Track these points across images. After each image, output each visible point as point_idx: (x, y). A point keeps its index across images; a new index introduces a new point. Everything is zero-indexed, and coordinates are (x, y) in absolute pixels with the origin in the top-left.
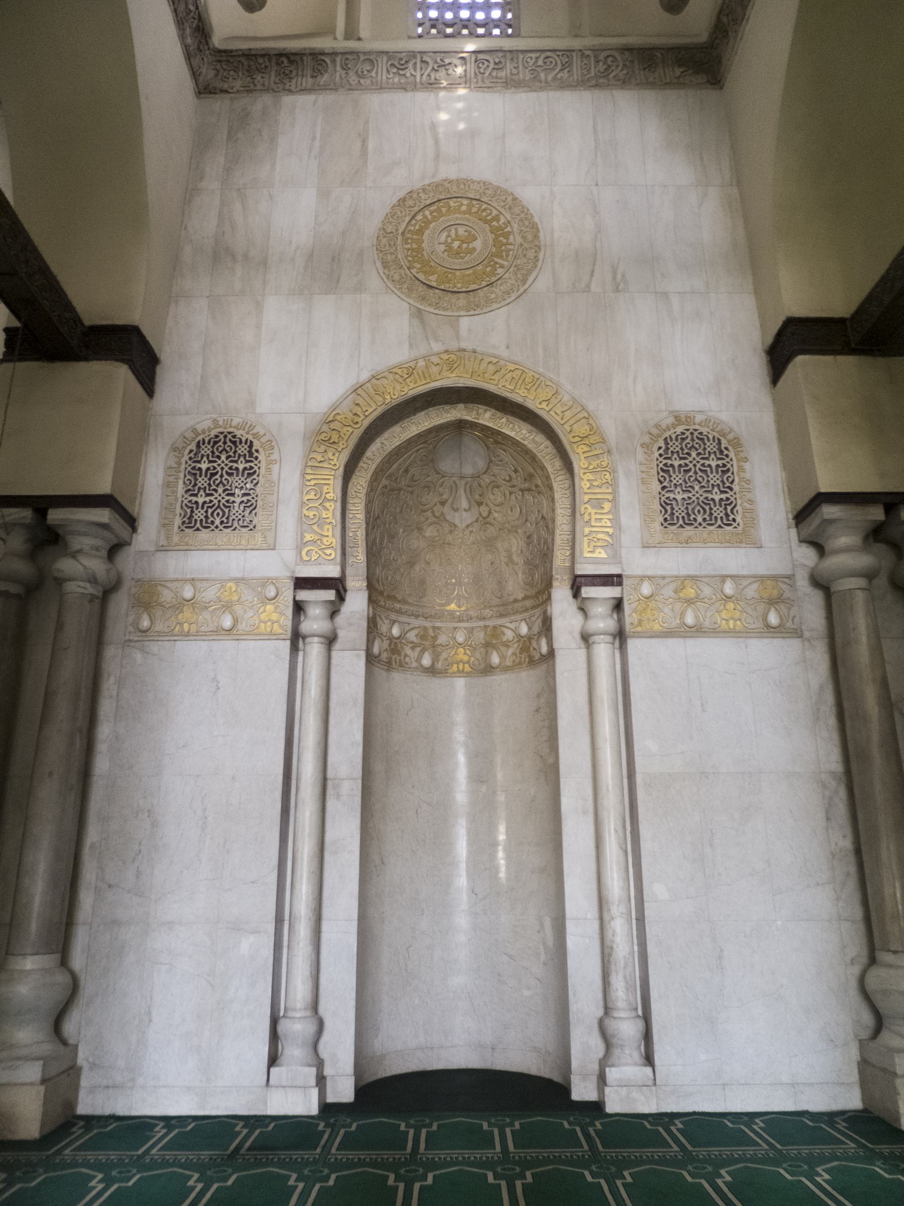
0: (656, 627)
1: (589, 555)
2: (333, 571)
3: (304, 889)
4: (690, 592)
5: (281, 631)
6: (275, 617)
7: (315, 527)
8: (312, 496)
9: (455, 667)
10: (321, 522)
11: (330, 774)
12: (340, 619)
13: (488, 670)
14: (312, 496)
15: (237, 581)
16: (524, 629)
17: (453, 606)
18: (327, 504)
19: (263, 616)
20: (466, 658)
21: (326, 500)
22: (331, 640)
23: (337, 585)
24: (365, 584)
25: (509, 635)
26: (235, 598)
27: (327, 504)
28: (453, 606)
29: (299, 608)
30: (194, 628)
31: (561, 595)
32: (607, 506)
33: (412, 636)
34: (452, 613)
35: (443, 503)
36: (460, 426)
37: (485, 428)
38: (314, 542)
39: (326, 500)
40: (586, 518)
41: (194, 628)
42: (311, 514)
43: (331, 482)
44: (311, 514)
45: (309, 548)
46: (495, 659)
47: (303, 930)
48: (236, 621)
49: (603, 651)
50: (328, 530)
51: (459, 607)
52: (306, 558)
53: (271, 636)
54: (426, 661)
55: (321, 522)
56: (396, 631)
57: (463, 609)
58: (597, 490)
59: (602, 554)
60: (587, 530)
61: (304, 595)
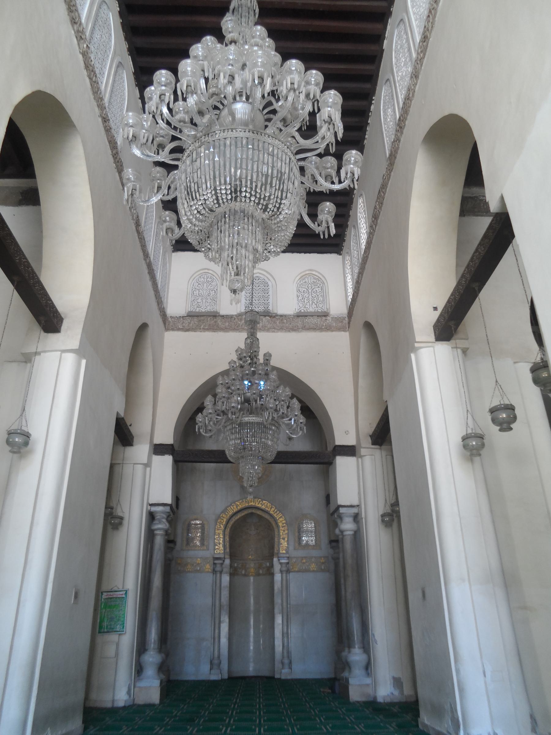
0: (296, 570)
1: (281, 552)
2: (222, 556)
3: (217, 631)
4: (304, 561)
5: (210, 571)
6: (209, 567)
7: (218, 545)
8: (217, 536)
9: (251, 574)
10: (220, 544)
11: (222, 604)
12: (224, 566)
13: (258, 575)
14: (217, 536)
15: (200, 558)
16: (268, 564)
17: (250, 557)
18: (221, 539)
19: (207, 567)
20: (253, 572)
21: (220, 538)
22: (221, 572)
23: (223, 559)
24: (229, 557)
25: (264, 565)
26: (200, 562)
27: (221, 539)
28: (250, 557)
29: (214, 564)
30: (191, 570)
31: (275, 559)
32: (286, 539)
33: (240, 566)
34: (250, 559)
35: (248, 529)
36: (252, 514)
37: (259, 515)
38: (217, 549)
39: (220, 538)
40: (281, 542)
41: (191, 570)
42: (217, 541)
43: (222, 533)
44: (217, 541)
45: (216, 550)
46: (261, 572)
47: (217, 640)
48: (200, 569)
49: (284, 575)
50: (221, 546)
51: (252, 557)
52: (216, 552)
53: (208, 572)
54: (243, 572)
55: (220, 544)
56: (236, 565)
57: (253, 557)
58: (284, 535)
59: (284, 552)
60: (281, 545)
61: (216, 562)
